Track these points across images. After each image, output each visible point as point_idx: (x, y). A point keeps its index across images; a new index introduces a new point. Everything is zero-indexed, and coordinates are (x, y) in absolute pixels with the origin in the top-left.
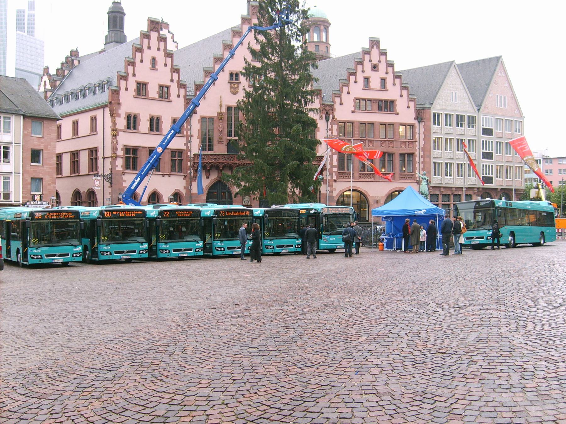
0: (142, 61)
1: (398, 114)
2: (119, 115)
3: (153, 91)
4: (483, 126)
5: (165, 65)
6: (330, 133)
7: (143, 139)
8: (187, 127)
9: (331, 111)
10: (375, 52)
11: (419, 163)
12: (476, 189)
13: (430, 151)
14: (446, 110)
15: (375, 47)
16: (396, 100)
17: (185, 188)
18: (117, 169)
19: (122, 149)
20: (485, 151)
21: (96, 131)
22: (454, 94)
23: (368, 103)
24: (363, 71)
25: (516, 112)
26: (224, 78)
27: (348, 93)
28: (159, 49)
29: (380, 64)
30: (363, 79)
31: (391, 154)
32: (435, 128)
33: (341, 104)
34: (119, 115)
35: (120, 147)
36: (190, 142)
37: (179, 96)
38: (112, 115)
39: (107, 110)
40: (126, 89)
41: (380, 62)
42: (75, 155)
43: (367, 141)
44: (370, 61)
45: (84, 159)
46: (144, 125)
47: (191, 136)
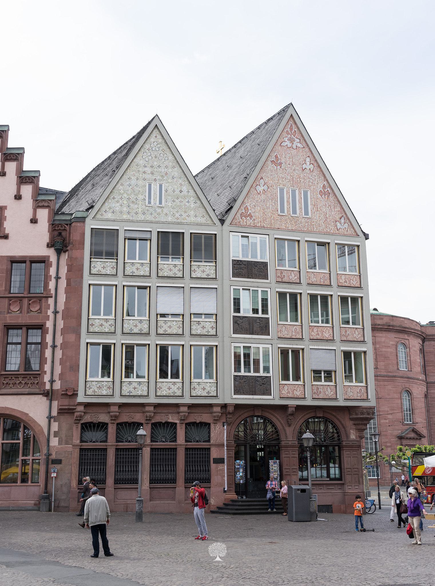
1: (6, 237)
11: (54, 347)
16: (5, 207)
22: (155, 188)
25: (343, 226)
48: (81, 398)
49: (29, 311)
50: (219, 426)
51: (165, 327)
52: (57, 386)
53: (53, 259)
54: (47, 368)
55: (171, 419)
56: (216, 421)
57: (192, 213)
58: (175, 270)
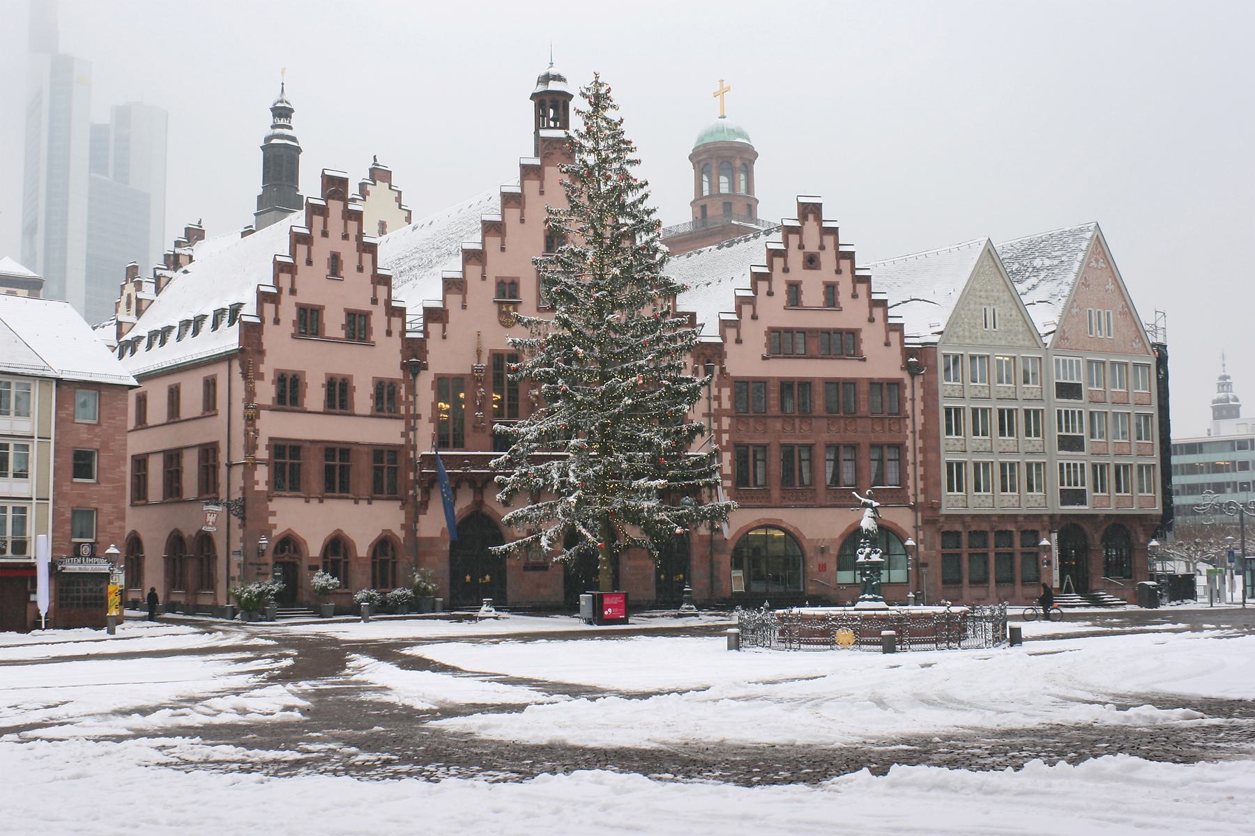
0: (309, 262)
1: (864, 360)
2: (261, 377)
3: (334, 324)
4: (1058, 377)
5: (360, 269)
6: (715, 405)
7: (311, 426)
8: (407, 398)
9: (717, 359)
10: (811, 227)
11: (914, 464)
12: (1046, 519)
13: (938, 438)
14: (973, 346)
15: (811, 217)
16: (860, 330)
17: (403, 527)
18: (257, 488)
19: (268, 447)
20: (1064, 433)
21: (214, 408)
23: (800, 338)
24: (786, 270)
26: (483, 294)
27: (754, 317)
28: (345, 237)
29: (822, 253)
30: (785, 287)
31: (854, 447)
32: (946, 386)
33: (738, 341)
34: (261, 377)
35: (263, 442)
36: (414, 429)
37: (389, 333)
38: (245, 376)
39: (236, 365)
40: (277, 321)
41: (822, 247)
42: (173, 458)
43: (797, 421)
44: (801, 247)
45: (190, 464)
46: (315, 396)
47: (418, 417)
48: (944, 511)
49: (890, 430)
50: (1046, 533)
51: (1004, 446)
52: (921, 498)
53: (907, 381)
54: (910, 483)
55: (1011, 527)
56: (1044, 529)
57: (1020, 336)
58: (1009, 392)
